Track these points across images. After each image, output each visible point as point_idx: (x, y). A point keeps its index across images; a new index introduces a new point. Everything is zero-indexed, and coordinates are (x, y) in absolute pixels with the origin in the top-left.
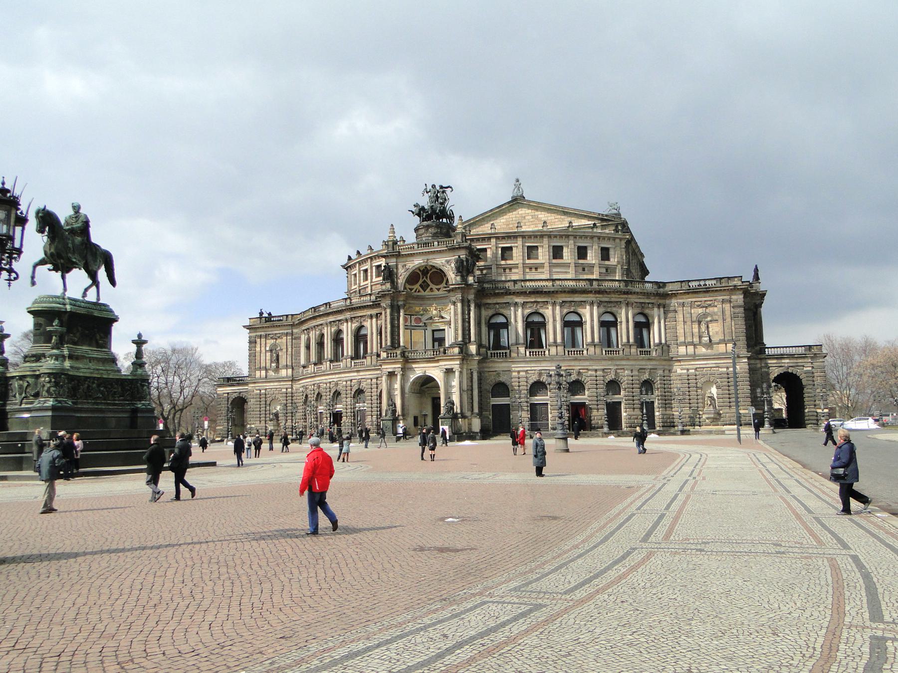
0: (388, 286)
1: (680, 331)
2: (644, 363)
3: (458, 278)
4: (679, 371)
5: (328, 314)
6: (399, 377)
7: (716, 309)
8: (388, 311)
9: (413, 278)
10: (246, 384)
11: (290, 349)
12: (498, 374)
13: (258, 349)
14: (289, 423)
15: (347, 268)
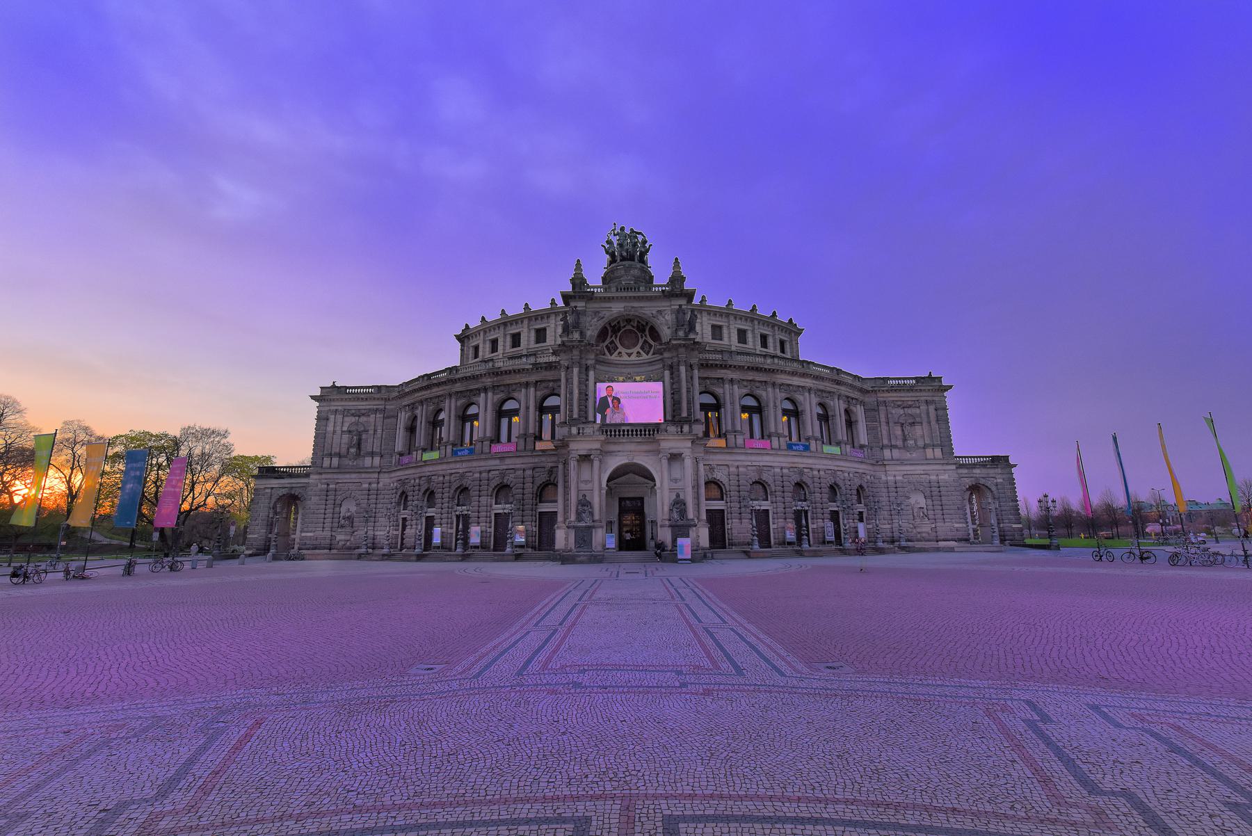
0: (576, 336)
1: (884, 432)
2: (857, 465)
3: (681, 334)
4: (884, 478)
5: (454, 381)
6: (596, 463)
7: (918, 411)
8: (576, 370)
9: (603, 334)
10: (307, 475)
11: (379, 431)
12: (712, 469)
13: (330, 428)
14: (370, 533)
15: (462, 338)
